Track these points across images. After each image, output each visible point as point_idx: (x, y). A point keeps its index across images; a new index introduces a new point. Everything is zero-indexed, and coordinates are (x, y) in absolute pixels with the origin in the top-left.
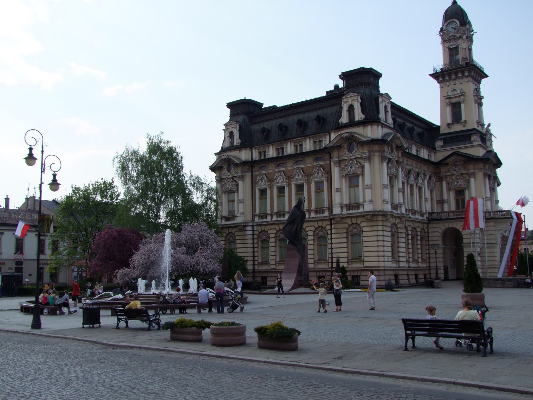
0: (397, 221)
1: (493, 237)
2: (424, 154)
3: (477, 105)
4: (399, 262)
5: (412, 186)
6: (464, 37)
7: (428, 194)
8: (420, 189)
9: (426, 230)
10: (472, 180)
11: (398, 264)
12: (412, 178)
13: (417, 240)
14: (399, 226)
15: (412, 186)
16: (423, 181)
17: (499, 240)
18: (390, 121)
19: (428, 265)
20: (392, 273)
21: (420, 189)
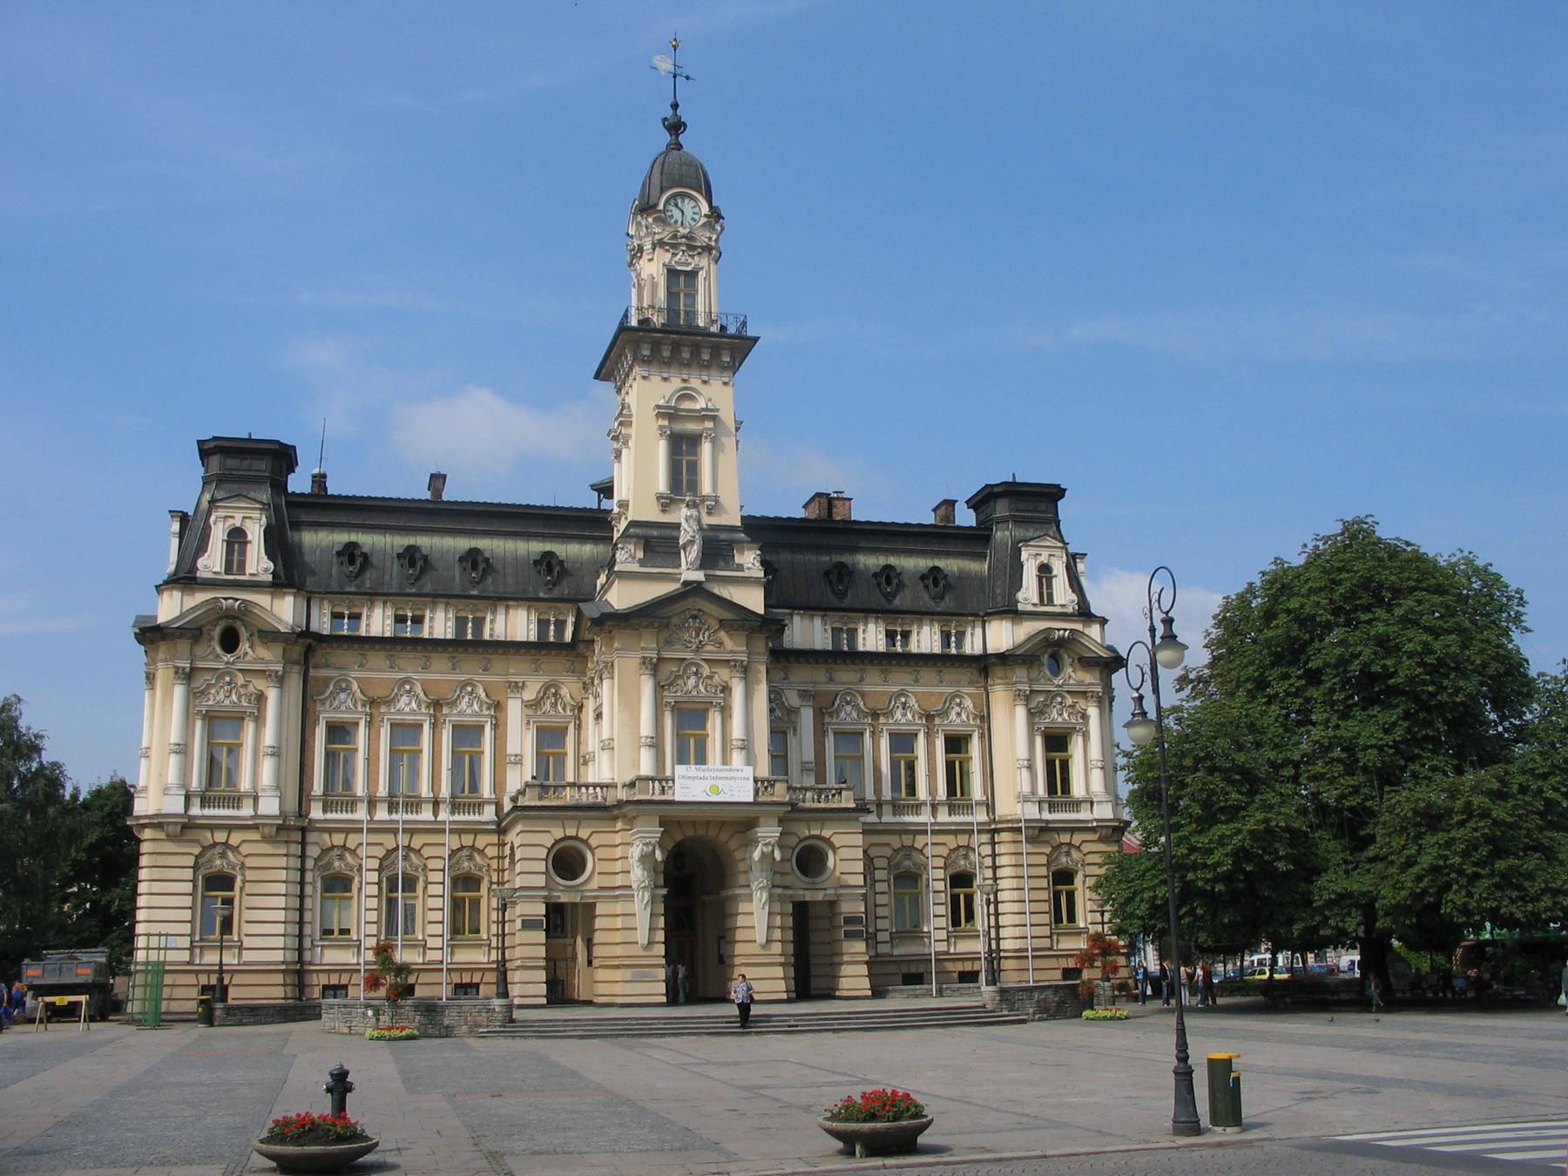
0: (235, 839)
1: (618, 866)
2: (517, 624)
3: (662, 447)
4: (241, 948)
5: (405, 732)
6: (648, 247)
7: (521, 739)
8: (467, 734)
9: (491, 852)
10: (605, 682)
11: (240, 954)
12: (407, 707)
13: (427, 883)
14: (245, 849)
15: (405, 732)
16: (498, 706)
17: (638, 875)
18: (258, 563)
19: (494, 957)
20: (191, 979)
21: (467, 734)
